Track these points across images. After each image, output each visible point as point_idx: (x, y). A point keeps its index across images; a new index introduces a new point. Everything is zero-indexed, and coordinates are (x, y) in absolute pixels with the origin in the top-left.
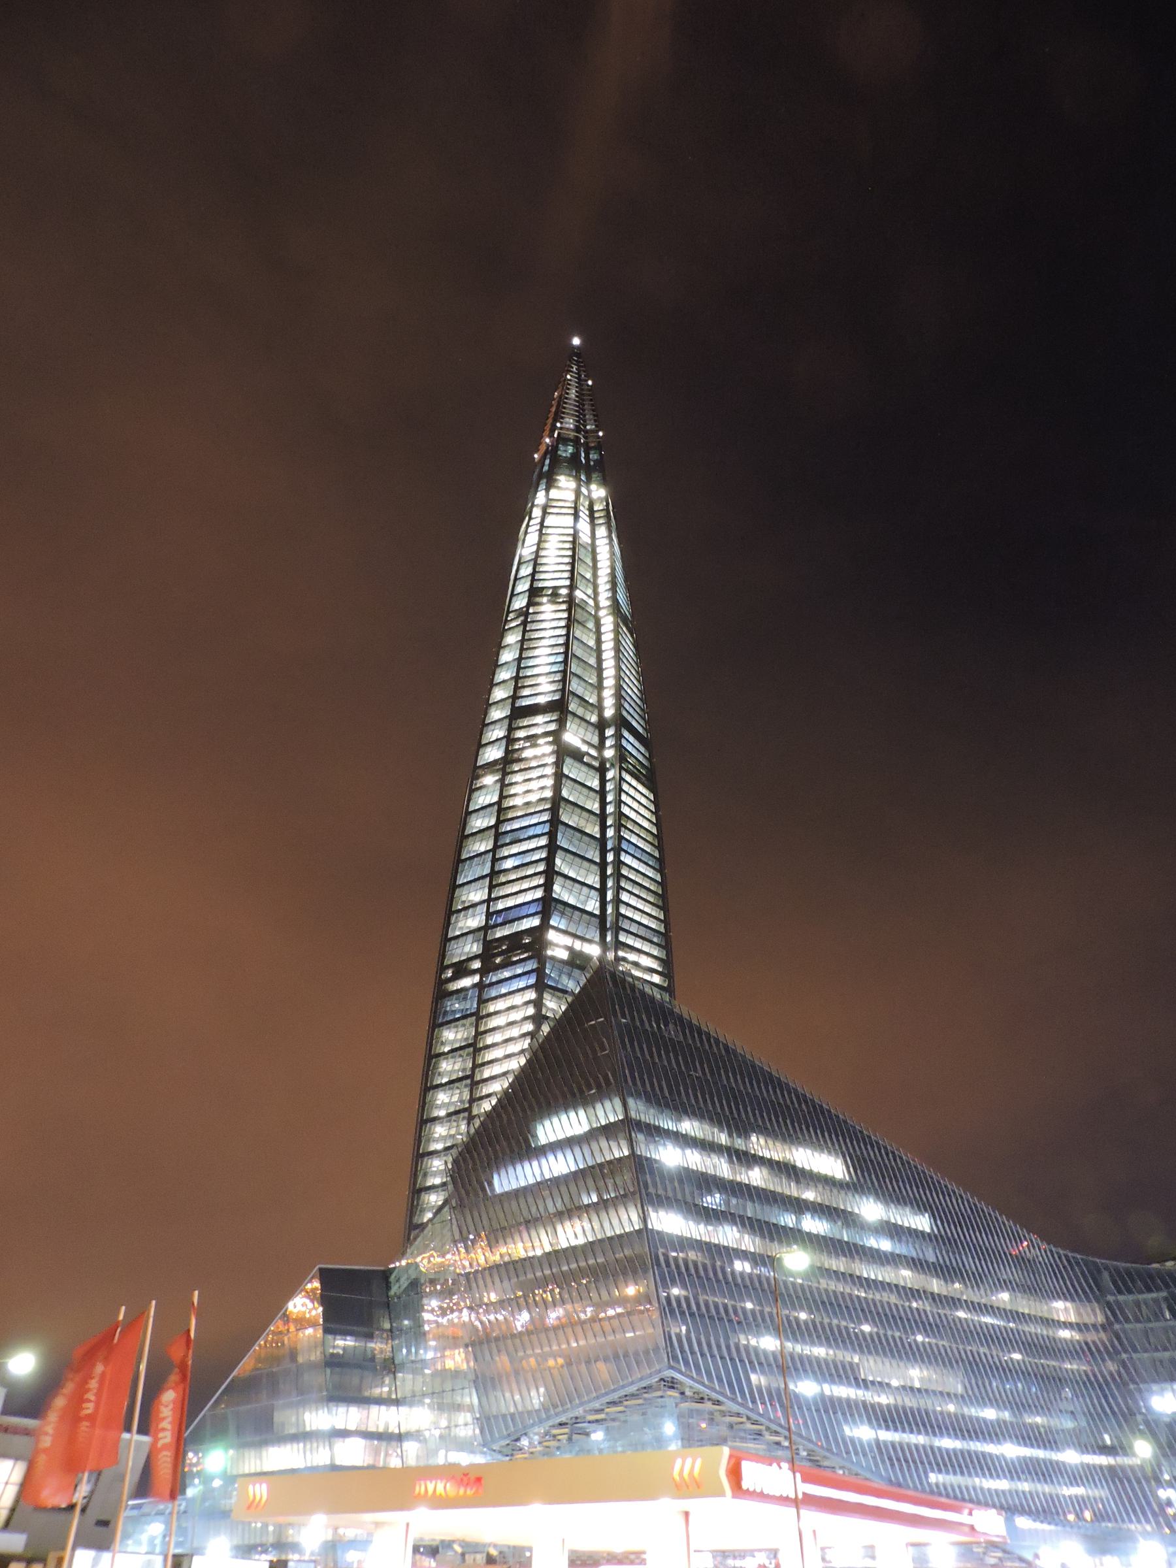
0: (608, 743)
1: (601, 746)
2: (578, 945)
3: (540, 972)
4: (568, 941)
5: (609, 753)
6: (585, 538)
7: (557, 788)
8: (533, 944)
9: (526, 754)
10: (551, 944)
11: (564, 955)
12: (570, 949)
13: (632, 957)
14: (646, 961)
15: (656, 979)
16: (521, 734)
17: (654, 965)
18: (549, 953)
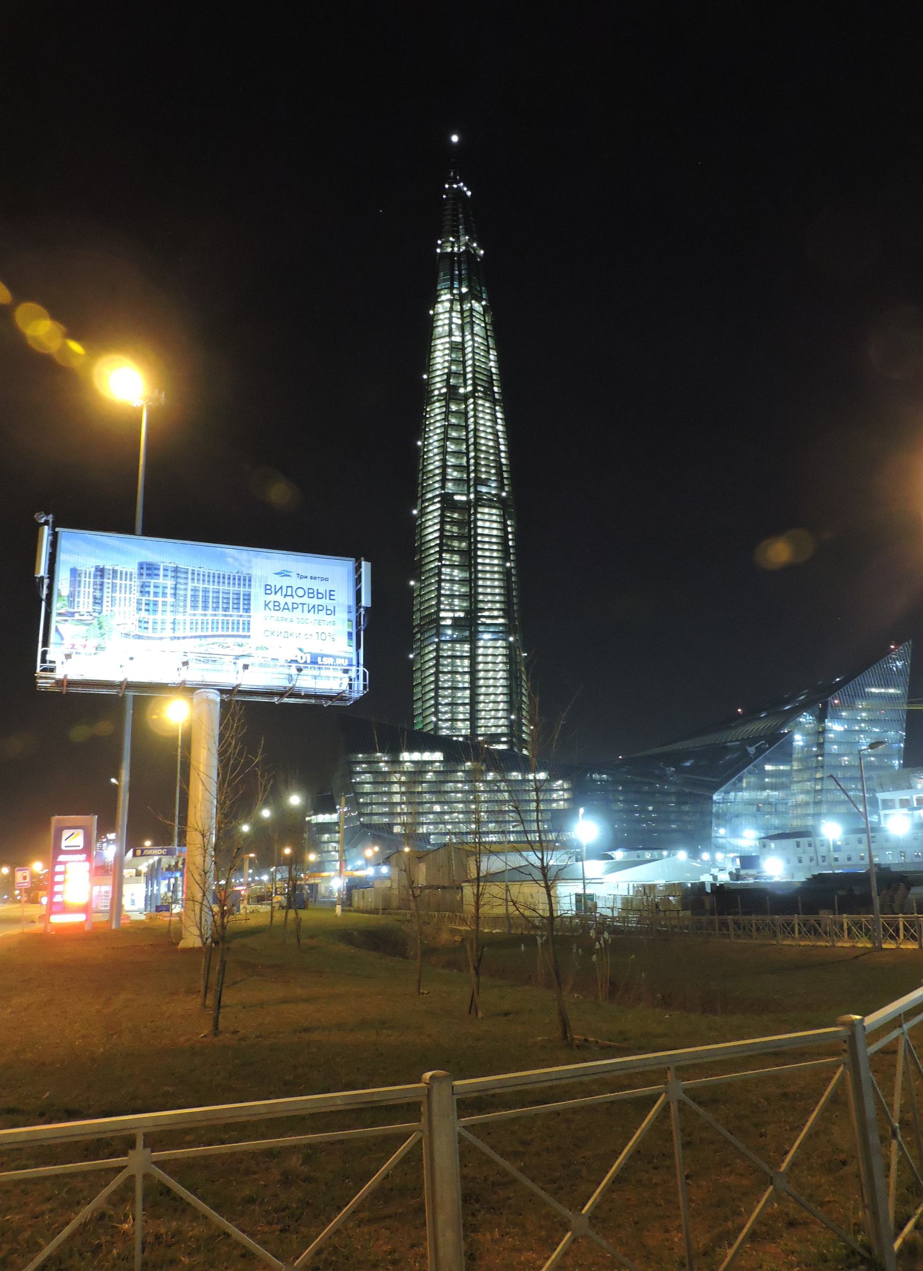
0: (472, 489)
1: (468, 495)
2: (457, 615)
3: (438, 635)
4: (451, 614)
5: (472, 496)
6: (458, 339)
7: (442, 530)
8: (435, 621)
9: (431, 508)
10: (444, 618)
11: (449, 622)
12: (454, 619)
13: (486, 613)
14: (496, 613)
15: (501, 621)
16: (430, 495)
17: (501, 613)
18: (443, 623)
